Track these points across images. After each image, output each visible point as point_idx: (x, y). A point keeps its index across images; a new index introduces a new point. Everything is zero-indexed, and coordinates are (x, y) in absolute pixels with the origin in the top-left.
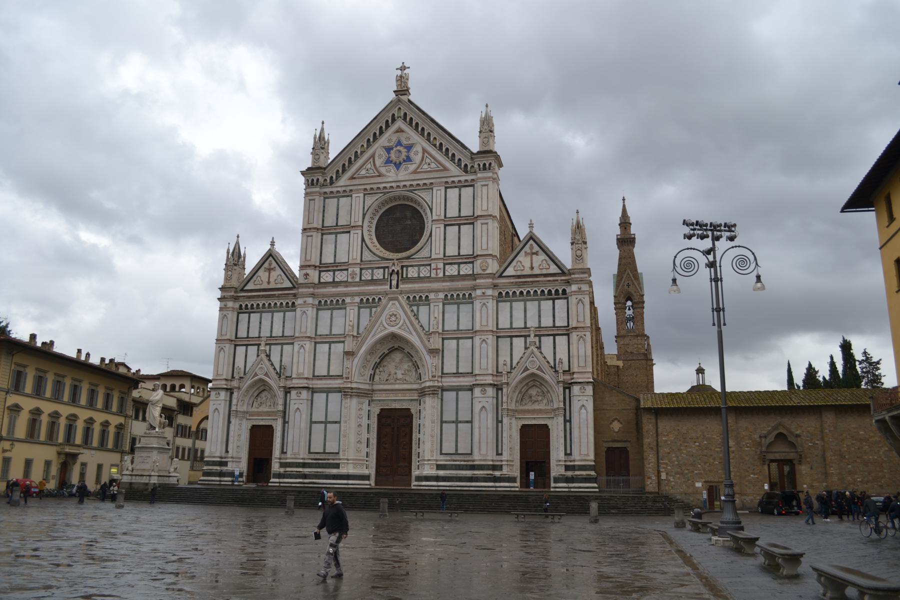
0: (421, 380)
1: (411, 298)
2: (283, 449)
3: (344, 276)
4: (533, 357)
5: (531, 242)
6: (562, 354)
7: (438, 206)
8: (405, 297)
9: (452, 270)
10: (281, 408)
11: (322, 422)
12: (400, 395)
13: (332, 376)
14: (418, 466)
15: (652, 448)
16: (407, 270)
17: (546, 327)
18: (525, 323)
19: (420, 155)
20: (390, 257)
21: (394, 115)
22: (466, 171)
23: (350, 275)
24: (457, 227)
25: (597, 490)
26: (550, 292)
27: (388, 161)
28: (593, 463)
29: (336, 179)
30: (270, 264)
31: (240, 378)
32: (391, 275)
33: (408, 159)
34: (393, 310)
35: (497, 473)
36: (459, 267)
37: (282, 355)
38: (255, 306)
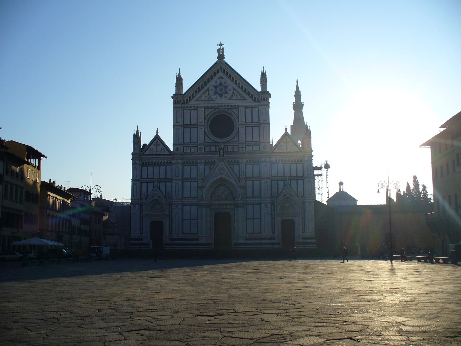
0: (235, 199)
1: (230, 161)
2: (169, 232)
4: (288, 190)
6: (300, 189)
8: (227, 161)
12: (224, 206)
14: (235, 239)
16: (227, 148)
19: (232, 91)
20: (218, 141)
21: (218, 70)
23: (199, 149)
24: (251, 127)
25: (316, 247)
27: (216, 93)
28: (314, 236)
29: (190, 101)
30: (157, 142)
31: (145, 198)
32: (220, 150)
33: (226, 93)
34: (221, 166)
35: (273, 241)
36: (252, 147)
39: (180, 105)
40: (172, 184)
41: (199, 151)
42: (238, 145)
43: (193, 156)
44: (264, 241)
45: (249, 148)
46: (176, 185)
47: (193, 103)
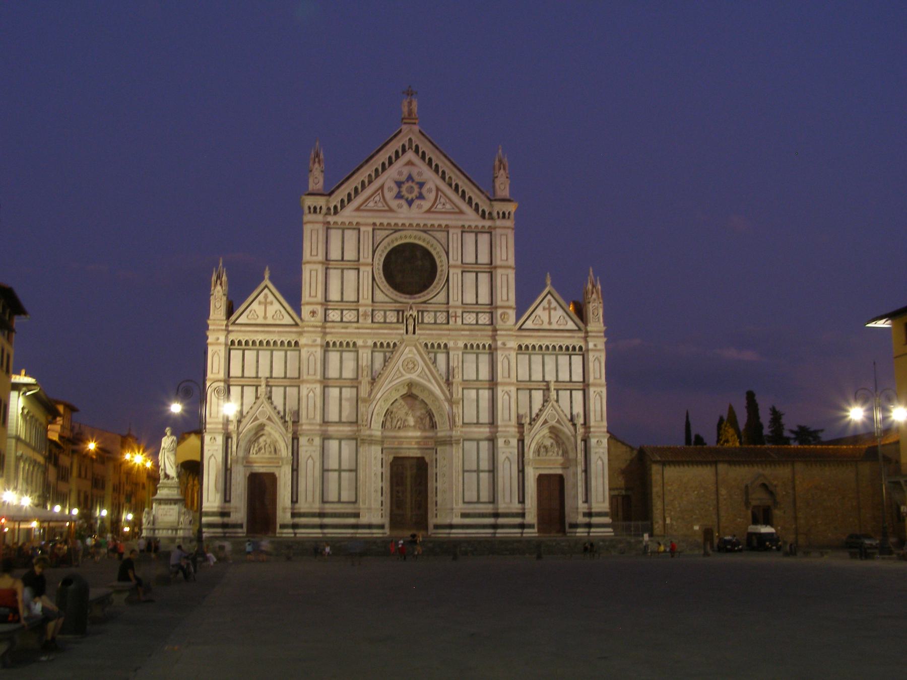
0: (436, 428)
3: (353, 316)
5: (549, 297)
7: (455, 249)
9: (470, 318)
10: (290, 454)
11: (335, 470)
13: (344, 423)
15: (659, 497)
17: (564, 382)
18: (544, 376)
19: (434, 193)
21: (404, 146)
22: (483, 216)
23: (363, 315)
24: (474, 274)
25: (613, 534)
26: (567, 348)
27: (399, 196)
30: (266, 297)
33: (421, 197)
34: (410, 355)
36: (477, 315)
37: (285, 398)
38: (251, 343)
39: (320, 218)
40: (299, 393)
41: (360, 320)
42: (444, 311)
43: (348, 331)
44: (501, 521)
45: (470, 318)
46: (309, 392)
47: (348, 215)
